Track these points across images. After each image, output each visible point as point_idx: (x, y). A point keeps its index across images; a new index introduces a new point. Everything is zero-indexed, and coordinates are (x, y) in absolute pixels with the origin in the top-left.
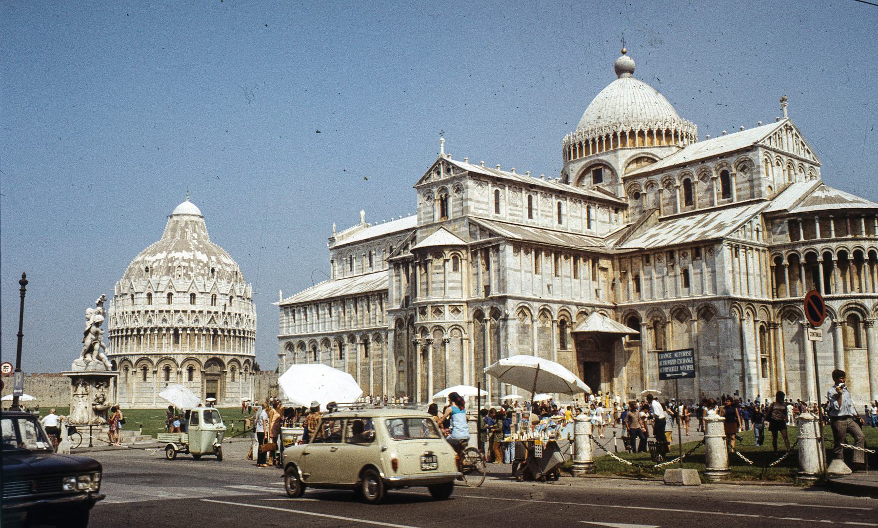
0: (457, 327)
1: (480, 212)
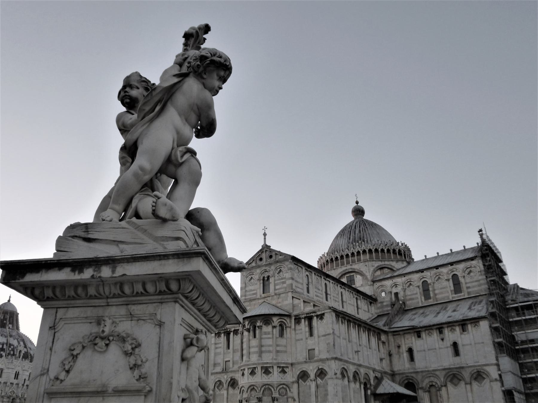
0: (285, 387)
1: (298, 290)
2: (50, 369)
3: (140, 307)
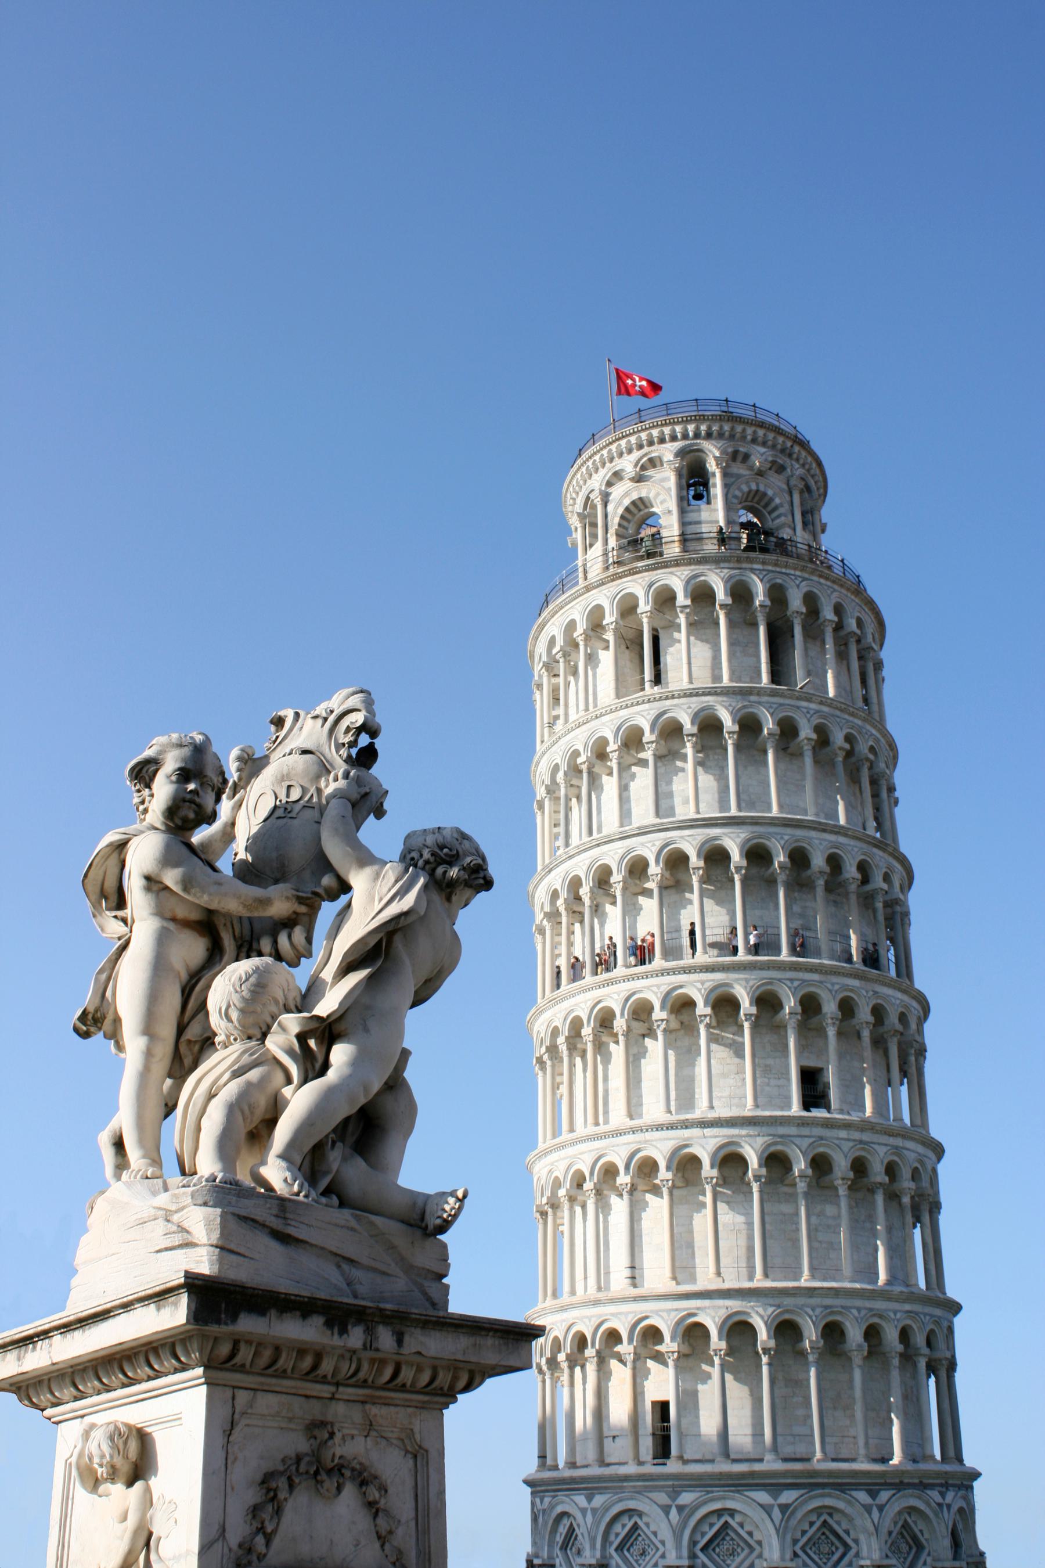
2: (227, 1526)
3: (384, 1410)
